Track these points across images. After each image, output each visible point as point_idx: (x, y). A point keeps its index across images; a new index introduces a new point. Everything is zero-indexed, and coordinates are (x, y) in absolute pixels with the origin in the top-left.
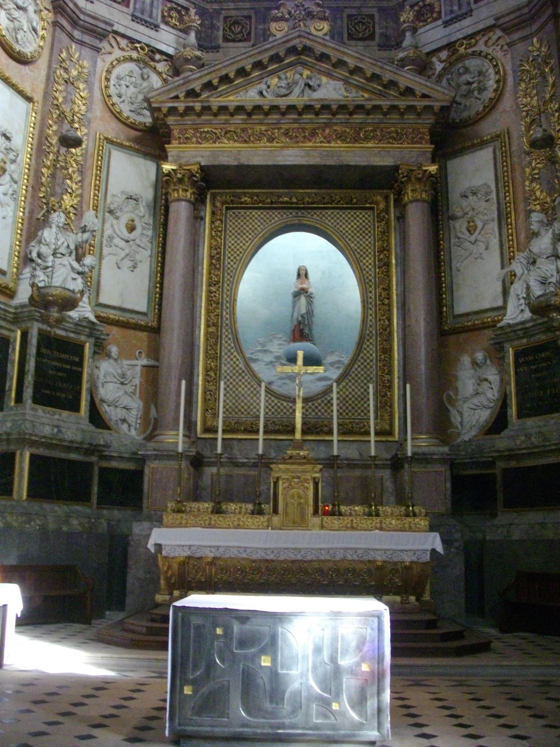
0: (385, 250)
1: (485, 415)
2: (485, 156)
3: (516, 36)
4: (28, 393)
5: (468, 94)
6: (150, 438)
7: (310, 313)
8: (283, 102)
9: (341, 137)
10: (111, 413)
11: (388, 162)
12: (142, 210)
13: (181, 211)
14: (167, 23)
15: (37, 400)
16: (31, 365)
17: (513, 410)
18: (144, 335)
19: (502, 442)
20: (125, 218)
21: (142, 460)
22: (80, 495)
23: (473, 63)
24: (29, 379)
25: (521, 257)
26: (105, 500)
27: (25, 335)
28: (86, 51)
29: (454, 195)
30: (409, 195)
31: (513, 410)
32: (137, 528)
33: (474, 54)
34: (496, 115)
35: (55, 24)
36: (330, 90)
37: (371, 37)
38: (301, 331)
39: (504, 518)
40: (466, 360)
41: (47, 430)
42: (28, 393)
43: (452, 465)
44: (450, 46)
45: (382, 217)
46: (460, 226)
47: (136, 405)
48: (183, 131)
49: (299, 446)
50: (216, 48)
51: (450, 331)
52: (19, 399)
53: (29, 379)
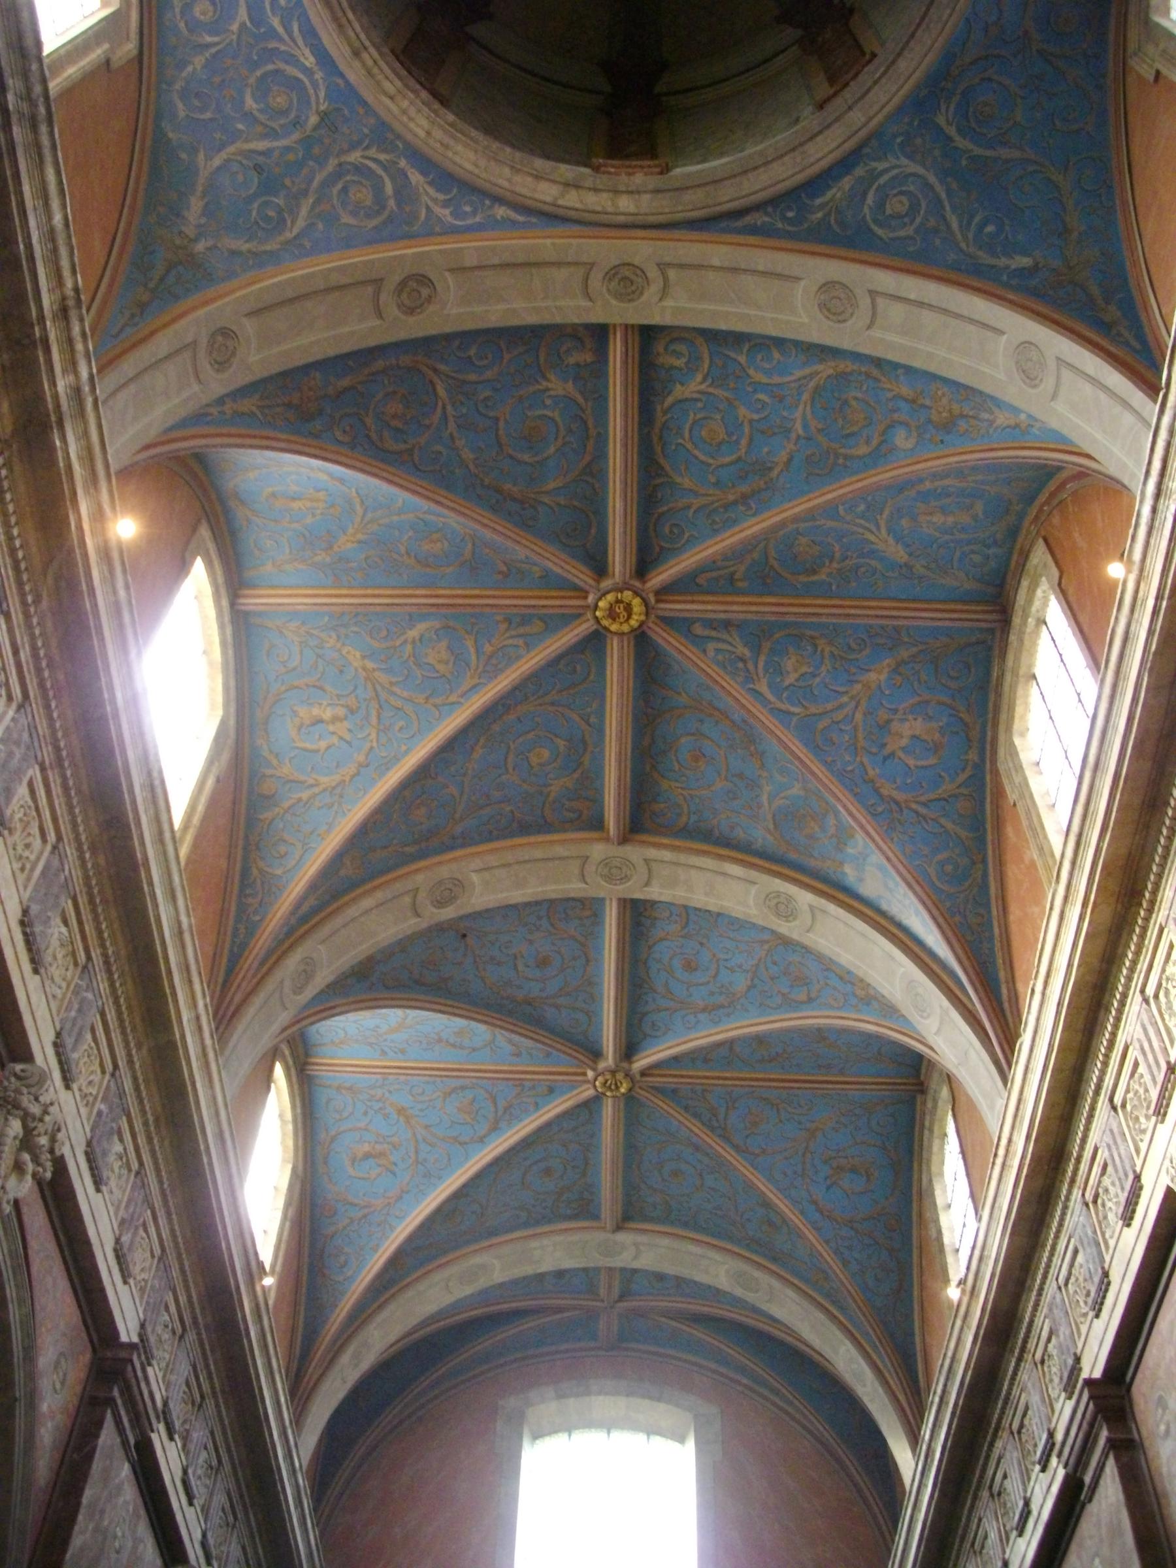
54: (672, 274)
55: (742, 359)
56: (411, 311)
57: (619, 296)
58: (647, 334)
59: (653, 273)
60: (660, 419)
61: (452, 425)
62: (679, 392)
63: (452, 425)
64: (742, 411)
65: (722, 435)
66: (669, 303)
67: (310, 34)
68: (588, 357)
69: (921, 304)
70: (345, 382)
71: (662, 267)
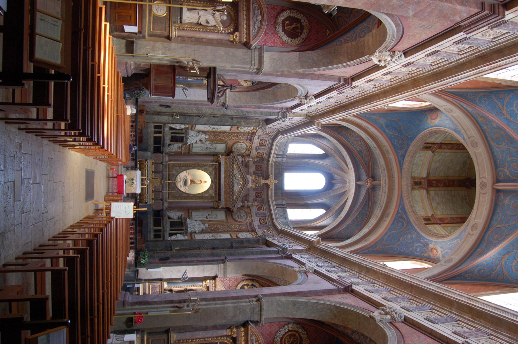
0: (205, 198)
1: (172, 216)
2: (224, 218)
3: (248, 225)
4: (173, 135)
5: (238, 216)
6: (167, 154)
7: (197, 184)
8: (234, 178)
9: (227, 190)
10: (171, 146)
11: (222, 199)
12: (213, 150)
13: (212, 158)
14: (258, 153)
15: (172, 137)
16: (178, 135)
17: (171, 220)
18: (188, 151)
19: (166, 218)
20: (211, 147)
21: (162, 153)
22: (155, 143)
23: (245, 217)
24: (175, 135)
25: (200, 223)
26: (155, 147)
27: (183, 133)
28: (246, 138)
29: (217, 212)
30: (215, 203)
31: (171, 220)
32: (149, 154)
33: (247, 217)
34: (232, 220)
35: (249, 133)
36: (236, 188)
37: (256, 197)
38: (192, 182)
39: (152, 218)
40: (183, 213)
41: (166, 138)
42: (173, 135)
43: (162, 210)
44: (251, 213)
45: (212, 198)
46: (210, 213)
47: (174, 150)
48: (229, 159)
49: (164, 182)
50: (254, 163)
51: (189, 210)
52: (172, 133)
53: (175, 135)
54: (481, 176)
55: (499, 161)
56: (477, 229)
57: (486, 188)
58: (497, 181)
59: (481, 180)
60: (515, 178)
61: (506, 225)
62: (508, 174)
63: (506, 225)
64: (509, 159)
65: (514, 163)
66: (487, 177)
67: (453, 240)
68: (502, 194)
69: (464, 129)
70: (485, 245)
71: (480, 178)
